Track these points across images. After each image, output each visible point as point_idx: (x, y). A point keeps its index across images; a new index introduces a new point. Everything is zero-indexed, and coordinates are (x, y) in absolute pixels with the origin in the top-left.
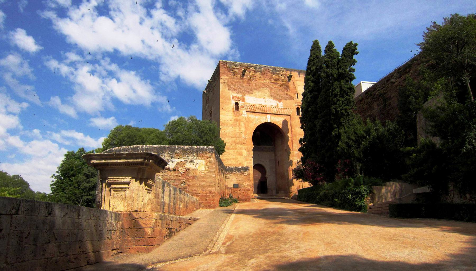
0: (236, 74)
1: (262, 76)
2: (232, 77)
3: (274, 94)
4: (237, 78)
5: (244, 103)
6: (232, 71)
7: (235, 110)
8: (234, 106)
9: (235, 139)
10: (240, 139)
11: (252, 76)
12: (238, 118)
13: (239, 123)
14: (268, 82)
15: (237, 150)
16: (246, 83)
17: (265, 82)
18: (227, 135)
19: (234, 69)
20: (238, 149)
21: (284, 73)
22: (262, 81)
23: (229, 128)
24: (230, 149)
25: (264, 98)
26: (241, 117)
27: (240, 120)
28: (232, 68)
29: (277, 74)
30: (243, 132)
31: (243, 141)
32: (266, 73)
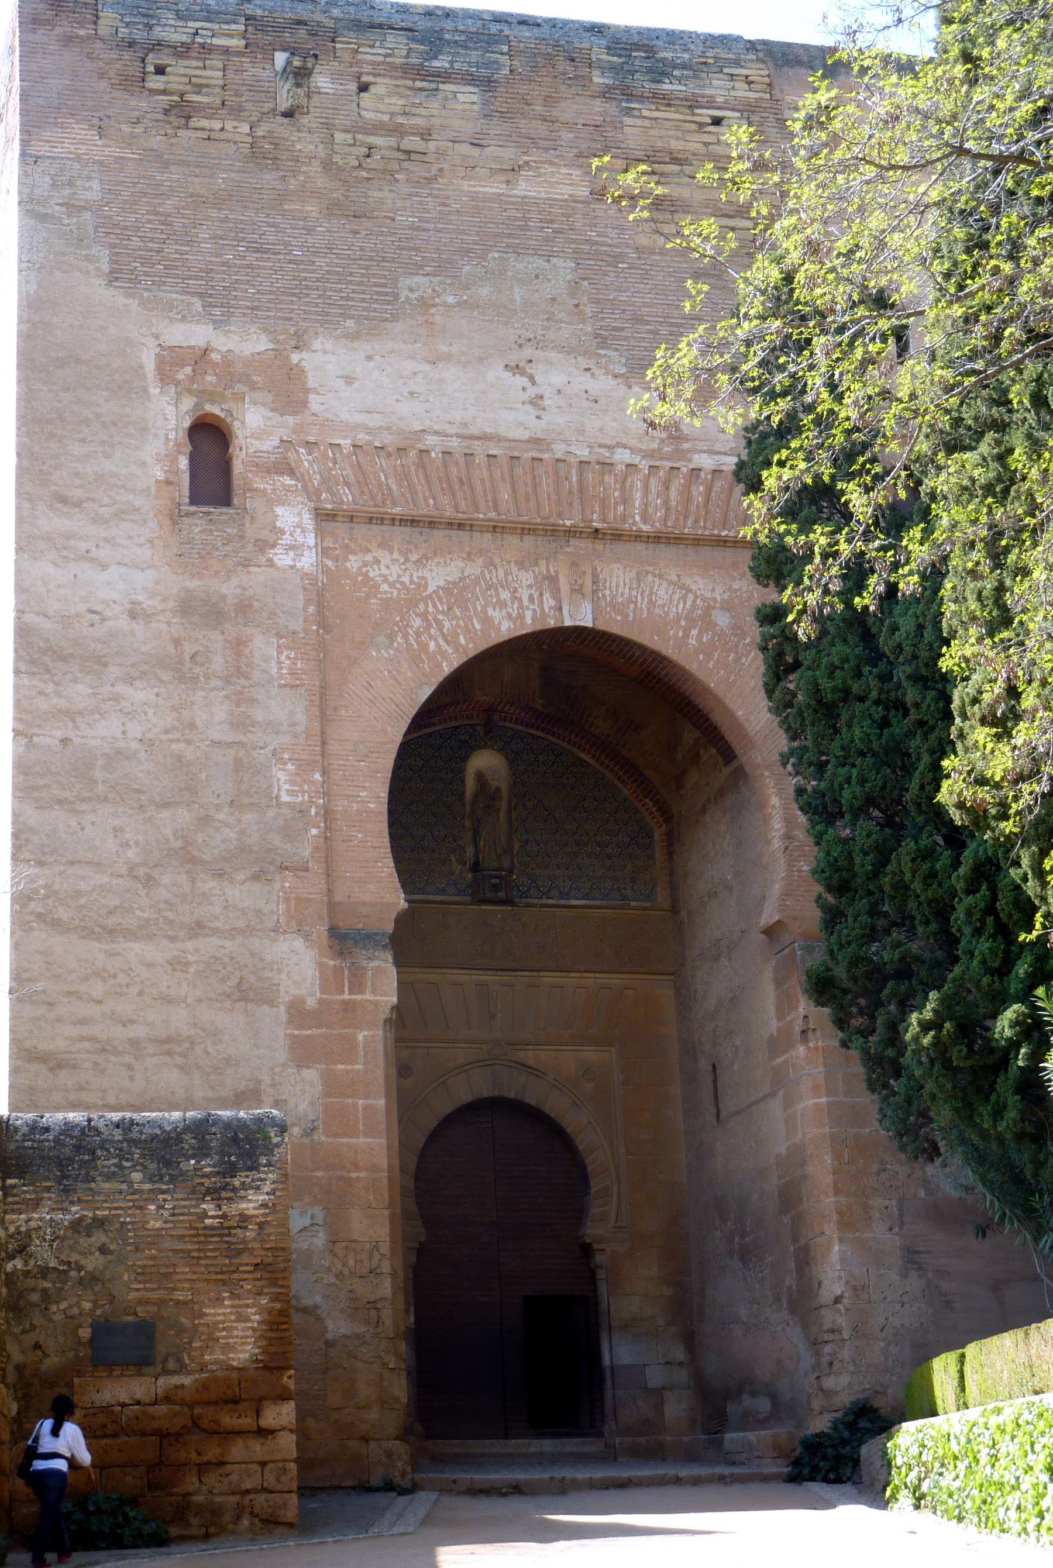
0: (200, 109)
1: (497, 128)
2: (156, 141)
3: (638, 320)
4: (212, 148)
5: (290, 420)
6: (155, 82)
7: (194, 500)
8: (184, 463)
9: (185, 816)
10: (248, 817)
11: (377, 128)
12: (229, 589)
13: (239, 645)
14: (564, 191)
15: (209, 945)
16: (312, 208)
17: (525, 187)
18: (98, 774)
19: (183, 51)
20: (215, 931)
21: (742, 92)
22: (494, 188)
23: (116, 698)
24: (130, 935)
25: (516, 369)
26: (258, 575)
27: (245, 608)
28: (158, 45)
29: (666, 101)
30: (286, 739)
31: (276, 840)
32: (548, 101)
